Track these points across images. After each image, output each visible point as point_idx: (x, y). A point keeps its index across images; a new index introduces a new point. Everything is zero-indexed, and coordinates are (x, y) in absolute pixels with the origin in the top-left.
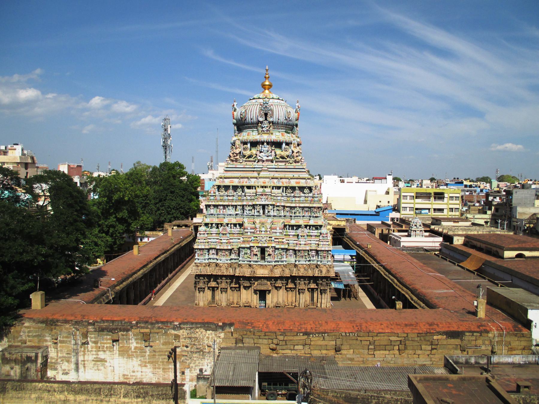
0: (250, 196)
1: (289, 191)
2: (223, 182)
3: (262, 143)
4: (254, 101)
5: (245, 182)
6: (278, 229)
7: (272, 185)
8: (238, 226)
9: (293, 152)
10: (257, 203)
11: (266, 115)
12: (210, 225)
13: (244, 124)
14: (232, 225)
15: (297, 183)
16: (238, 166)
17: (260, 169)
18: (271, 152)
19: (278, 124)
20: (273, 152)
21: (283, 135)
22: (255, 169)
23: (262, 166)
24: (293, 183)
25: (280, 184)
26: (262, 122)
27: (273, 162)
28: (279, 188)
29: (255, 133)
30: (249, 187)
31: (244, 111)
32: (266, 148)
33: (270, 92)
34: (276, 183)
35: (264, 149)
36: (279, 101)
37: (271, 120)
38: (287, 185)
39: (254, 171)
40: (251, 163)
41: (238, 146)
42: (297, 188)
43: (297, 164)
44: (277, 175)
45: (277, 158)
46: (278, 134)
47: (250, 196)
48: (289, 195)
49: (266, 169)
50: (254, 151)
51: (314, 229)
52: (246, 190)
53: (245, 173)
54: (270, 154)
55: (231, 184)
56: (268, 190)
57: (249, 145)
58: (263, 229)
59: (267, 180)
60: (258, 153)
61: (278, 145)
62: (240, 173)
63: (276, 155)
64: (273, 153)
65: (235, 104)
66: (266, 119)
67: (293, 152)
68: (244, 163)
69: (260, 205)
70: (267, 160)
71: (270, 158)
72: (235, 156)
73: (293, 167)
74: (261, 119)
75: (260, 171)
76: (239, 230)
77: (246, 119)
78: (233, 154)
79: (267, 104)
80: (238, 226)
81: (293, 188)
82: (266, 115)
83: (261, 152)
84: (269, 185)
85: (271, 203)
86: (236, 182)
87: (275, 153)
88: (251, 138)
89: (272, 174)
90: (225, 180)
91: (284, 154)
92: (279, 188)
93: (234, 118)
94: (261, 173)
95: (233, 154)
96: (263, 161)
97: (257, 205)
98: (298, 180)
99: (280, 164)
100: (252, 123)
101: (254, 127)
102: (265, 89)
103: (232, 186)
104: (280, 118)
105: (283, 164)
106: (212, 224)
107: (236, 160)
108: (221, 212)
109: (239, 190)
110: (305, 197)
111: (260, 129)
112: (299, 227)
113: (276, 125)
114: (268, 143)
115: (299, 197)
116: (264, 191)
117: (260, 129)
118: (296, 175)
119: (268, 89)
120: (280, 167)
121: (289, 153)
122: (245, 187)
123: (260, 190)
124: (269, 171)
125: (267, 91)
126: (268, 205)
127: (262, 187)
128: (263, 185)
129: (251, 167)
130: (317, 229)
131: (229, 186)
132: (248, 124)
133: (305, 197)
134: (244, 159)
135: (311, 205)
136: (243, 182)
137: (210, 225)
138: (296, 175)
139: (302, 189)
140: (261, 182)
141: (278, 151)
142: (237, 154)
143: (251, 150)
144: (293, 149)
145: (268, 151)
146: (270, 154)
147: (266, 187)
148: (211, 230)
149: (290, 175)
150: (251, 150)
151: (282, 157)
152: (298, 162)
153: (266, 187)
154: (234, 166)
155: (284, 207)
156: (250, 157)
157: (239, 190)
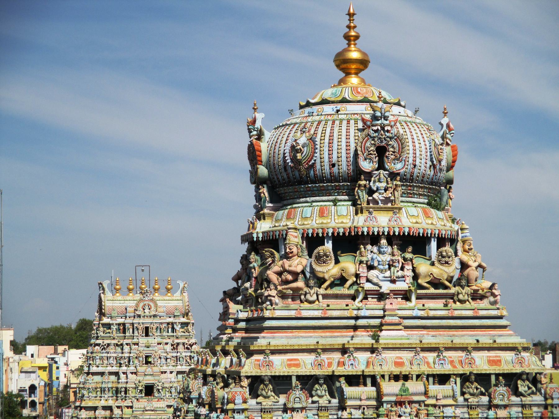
0: (359, 407)
1: (473, 387)
2: (270, 364)
3: (374, 239)
4: (328, 109)
5: (333, 364)
7: (425, 369)
9: (464, 266)
11: (381, 151)
13: (302, 181)
15: (492, 362)
16: (305, 314)
17: (377, 322)
18: (402, 269)
19: (412, 180)
20: (409, 267)
22: (361, 322)
23: (381, 313)
24: (481, 363)
25: (447, 369)
26: (369, 175)
28: (443, 379)
30: (354, 380)
31: (303, 140)
32: (384, 254)
34: (430, 363)
35: (381, 258)
37: (398, 167)
38: (467, 370)
39: (355, 328)
40: (342, 303)
41: (295, 250)
42: (294, 379)
43: (484, 303)
44: (430, 338)
45: (420, 287)
46: (413, 211)
47: (359, 407)
48: (473, 400)
49: (396, 320)
50: (349, 264)
52: (349, 391)
53: (328, 334)
54: (400, 273)
55: (294, 371)
56: (415, 387)
57: (329, 246)
59: (406, 356)
60: (363, 271)
61: (416, 243)
62: (319, 333)
63: (416, 277)
65: (259, 116)
66: (381, 166)
67: (464, 266)
68: (324, 303)
70: (396, 293)
71: (401, 286)
72: (287, 282)
73: (470, 313)
75: (380, 328)
78: (280, 274)
79: (386, 118)
81: (483, 379)
82: (381, 151)
83: (371, 268)
84: (415, 370)
86: (307, 365)
88: (333, 224)
89: (413, 337)
90: (272, 358)
92: (443, 379)
94: (384, 333)
95: (280, 274)
96: (381, 297)
98: (492, 354)
100: (334, 178)
101: (338, 190)
102: (348, 74)
103: (299, 377)
104: (417, 163)
105: (439, 304)
107: (296, 295)
109: (321, 390)
110: (523, 406)
111: (363, 196)
113: (409, 182)
114: (391, 239)
115: (505, 407)
117: (363, 196)
118: (485, 338)
120: (432, 313)
121: (453, 270)
122: (342, 380)
123: (391, 388)
124: (406, 327)
127: (396, 378)
128: (396, 371)
129: (346, 314)
131: (289, 378)
132: (321, 179)
133: (523, 406)
134: (322, 291)
136: (330, 364)
138: (485, 338)
139: (511, 380)
140: (387, 362)
141: (423, 266)
142: (295, 275)
143: (337, 262)
144: (465, 257)
146: (400, 273)
147: (406, 378)
149: (466, 338)
150: (337, 262)
151: (436, 283)
152: (482, 297)
153: (406, 378)
154: (293, 313)
156: (342, 280)
157: (321, 390)
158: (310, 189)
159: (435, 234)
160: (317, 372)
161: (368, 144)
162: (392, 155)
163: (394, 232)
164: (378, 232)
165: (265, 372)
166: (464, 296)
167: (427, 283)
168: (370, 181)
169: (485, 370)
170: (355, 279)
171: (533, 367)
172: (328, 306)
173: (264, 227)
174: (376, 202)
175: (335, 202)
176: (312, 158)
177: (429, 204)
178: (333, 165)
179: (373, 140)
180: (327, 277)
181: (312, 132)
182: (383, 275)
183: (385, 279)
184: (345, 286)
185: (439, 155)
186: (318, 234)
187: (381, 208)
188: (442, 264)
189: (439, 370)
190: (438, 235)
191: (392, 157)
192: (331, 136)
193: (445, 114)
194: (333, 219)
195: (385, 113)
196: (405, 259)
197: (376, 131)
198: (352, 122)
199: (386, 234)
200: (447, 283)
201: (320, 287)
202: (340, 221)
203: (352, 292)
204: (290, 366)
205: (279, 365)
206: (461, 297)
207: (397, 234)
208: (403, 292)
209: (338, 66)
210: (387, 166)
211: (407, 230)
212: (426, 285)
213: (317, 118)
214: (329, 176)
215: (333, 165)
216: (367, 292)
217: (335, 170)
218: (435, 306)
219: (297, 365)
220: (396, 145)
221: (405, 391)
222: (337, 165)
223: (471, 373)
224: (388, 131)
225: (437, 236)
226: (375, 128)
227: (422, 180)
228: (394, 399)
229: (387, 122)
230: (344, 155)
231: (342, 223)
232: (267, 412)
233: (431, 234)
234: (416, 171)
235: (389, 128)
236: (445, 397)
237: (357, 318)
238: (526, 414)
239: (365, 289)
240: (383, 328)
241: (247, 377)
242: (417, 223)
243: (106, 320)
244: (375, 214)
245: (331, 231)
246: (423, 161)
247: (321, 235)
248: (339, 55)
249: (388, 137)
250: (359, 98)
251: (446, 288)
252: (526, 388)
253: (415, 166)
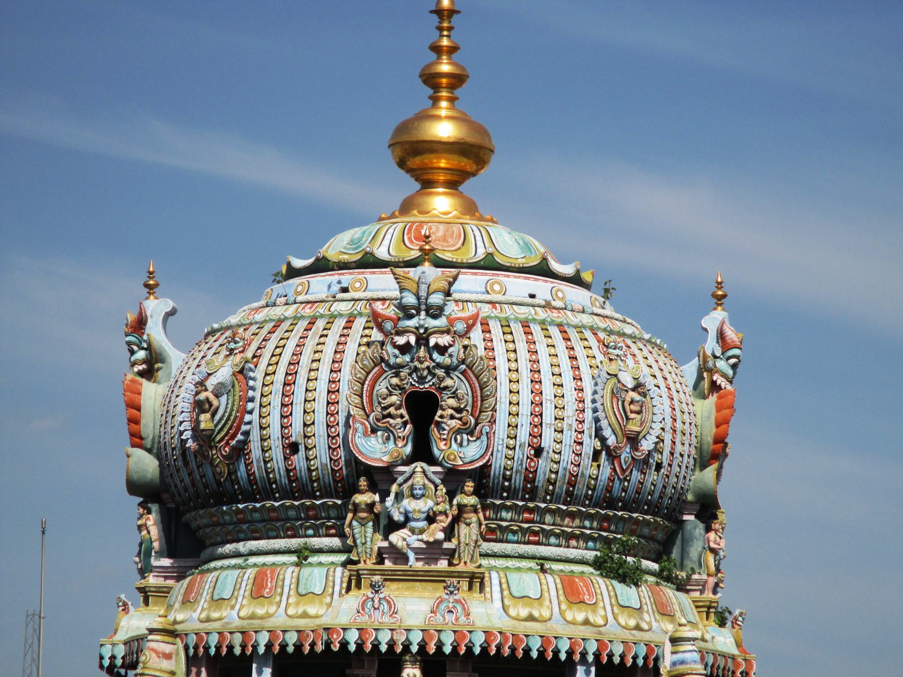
4: (320, 285)
11: (422, 408)
13: (225, 492)
19: (532, 493)
21: (573, 593)
26: (381, 478)
29: (323, 572)
31: (224, 374)
33: (470, 208)
36: (542, 287)
37: (469, 453)
46: (527, 581)
66: (422, 452)
74: (375, 450)
77: (241, 450)
79: (435, 312)
82: (422, 408)
88: (279, 620)
93: (137, 439)
100: (298, 487)
102: (427, 184)
104: (548, 440)
111: (369, 539)
113: (507, 499)
119: (453, 185)
125: (441, 203)
158: (243, 518)
161: (382, 387)
162: (452, 417)
163: (440, 645)
164: (391, 644)
168: (384, 495)
174: (400, 556)
175: (302, 555)
177: (597, 564)
178: (294, 448)
179: (397, 375)
181: (249, 354)
185: (628, 419)
187: (416, 573)
190: (597, 656)
191: (454, 423)
193: (720, 300)
195: (428, 295)
197: (405, 349)
209: (402, 164)
210: (436, 452)
214: (285, 480)
215: (294, 448)
217: (299, 461)
220: (464, 389)
222: (302, 448)
225: (590, 658)
226: (401, 340)
227: (569, 494)
230: (320, 417)
231: (305, 615)
234: (543, 466)
235: (444, 340)
242: (531, 618)
244: (391, 590)
246: (569, 437)
248: (404, 127)
249: (439, 366)
253: (539, 452)
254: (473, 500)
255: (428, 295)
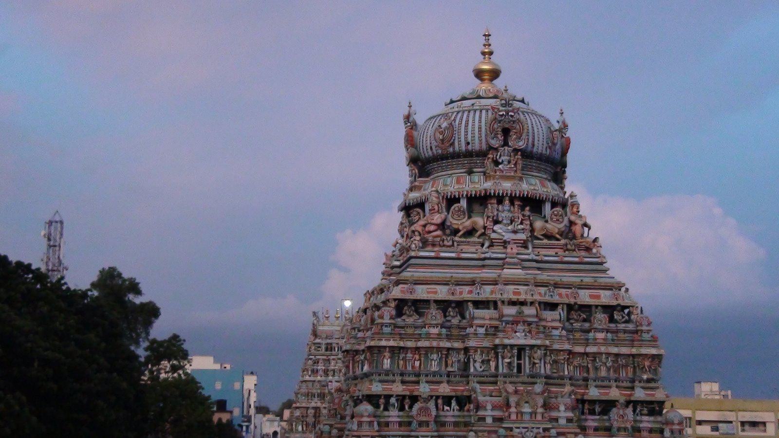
3: (500, 200)
5: (465, 293)
6: (562, 408)
7: (537, 297)
8: (454, 403)
10: (507, 341)
11: (506, 132)
12: (382, 401)
14: (440, 401)
15: (591, 296)
16: (443, 255)
21: (543, 185)
23: (503, 256)
25: (556, 299)
26: (496, 149)
27: (526, 247)
28: (553, 306)
30: (478, 304)
34: (542, 294)
50: (479, 221)
51: (645, 411)
54: (520, 227)
55: (432, 297)
56: (529, 311)
58: (527, 409)
59: (522, 288)
60: (489, 224)
64: (526, 225)
66: (506, 144)
69: (512, 346)
70: (515, 241)
74: (495, 143)
76: (457, 413)
80: (454, 403)
81: (586, 308)
82: (506, 132)
83: (496, 222)
84: (529, 298)
85: (539, 342)
86: (442, 293)
87: (531, 225)
88: (467, 188)
91: (554, 227)
92: (553, 306)
97: (505, 346)
99: (543, 252)
104: (536, 143)
106: (388, 397)
108: (409, 368)
112: (608, 406)
116: (520, 313)
122: (470, 305)
123: (510, 311)
126: (532, 347)
127: (512, 303)
128: (514, 298)
130: (651, 413)
135: (634, 351)
136: (461, 293)
137: (382, 401)
141: (538, 224)
144: (573, 218)
145: (512, 221)
148: (386, 413)
151: (549, 236)
153: (523, 303)
155: (570, 352)
159: (549, 199)
160: (451, 298)
161: (496, 126)
162: (514, 135)
163: (515, 194)
164: (503, 194)
165: (408, 296)
166: (571, 246)
167: (542, 235)
169: (587, 302)
170: (483, 231)
171: (627, 301)
172: (462, 250)
173: (415, 195)
176: (452, 136)
180: (461, 228)
181: (453, 118)
182: (506, 228)
183: (507, 231)
184: (475, 235)
186: (455, 196)
188: (554, 222)
189: (547, 299)
190: (552, 200)
191: (515, 136)
192: (467, 121)
194: (467, 185)
195: (509, 101)
196: (523, 215)
197: (502, 115)
198: (484, 112)
199: (509, 195)
200: (558, 236)
201: (455, 235)
202: (473, 186)
203: (481, 240)
204: (428, 293)
205: (421, 292)
206: (569, 247)
207: (518, 195)
208: (522, 242)
211: (526, 194)
212: (542, 237)
213: (457, 109)
215: (468, 143)
216: (493, 241)
217: (470, 147)
218: (549, 254)
219: (436, 293)
221: (520, 313)
223: (575, 303)
224: (512, 116)
225: (550, 200)
226: (501, 113)
228: (511, 319)
229: (510, 109)
232: (410, 327)
233: (546, 198)
235: (512, 114)
236: (553, 321)
237: (485, 259)
238: (620, 337)
239: (491, 237)
240: (505, 267)
241: (395, 300)
242: (535, 190)
243: (318, 341)
245: (465, 193)
246: (541, 143)
247: (457, 197)
250: (491, 95)
251: (558, 240)
252: (621, 317)
254: (520, 157)
255: (509, 101)
